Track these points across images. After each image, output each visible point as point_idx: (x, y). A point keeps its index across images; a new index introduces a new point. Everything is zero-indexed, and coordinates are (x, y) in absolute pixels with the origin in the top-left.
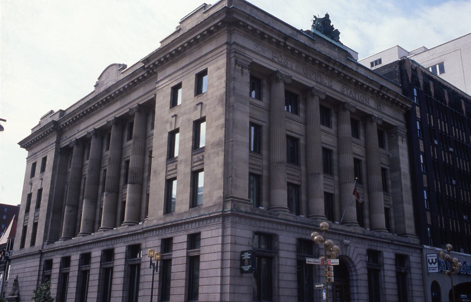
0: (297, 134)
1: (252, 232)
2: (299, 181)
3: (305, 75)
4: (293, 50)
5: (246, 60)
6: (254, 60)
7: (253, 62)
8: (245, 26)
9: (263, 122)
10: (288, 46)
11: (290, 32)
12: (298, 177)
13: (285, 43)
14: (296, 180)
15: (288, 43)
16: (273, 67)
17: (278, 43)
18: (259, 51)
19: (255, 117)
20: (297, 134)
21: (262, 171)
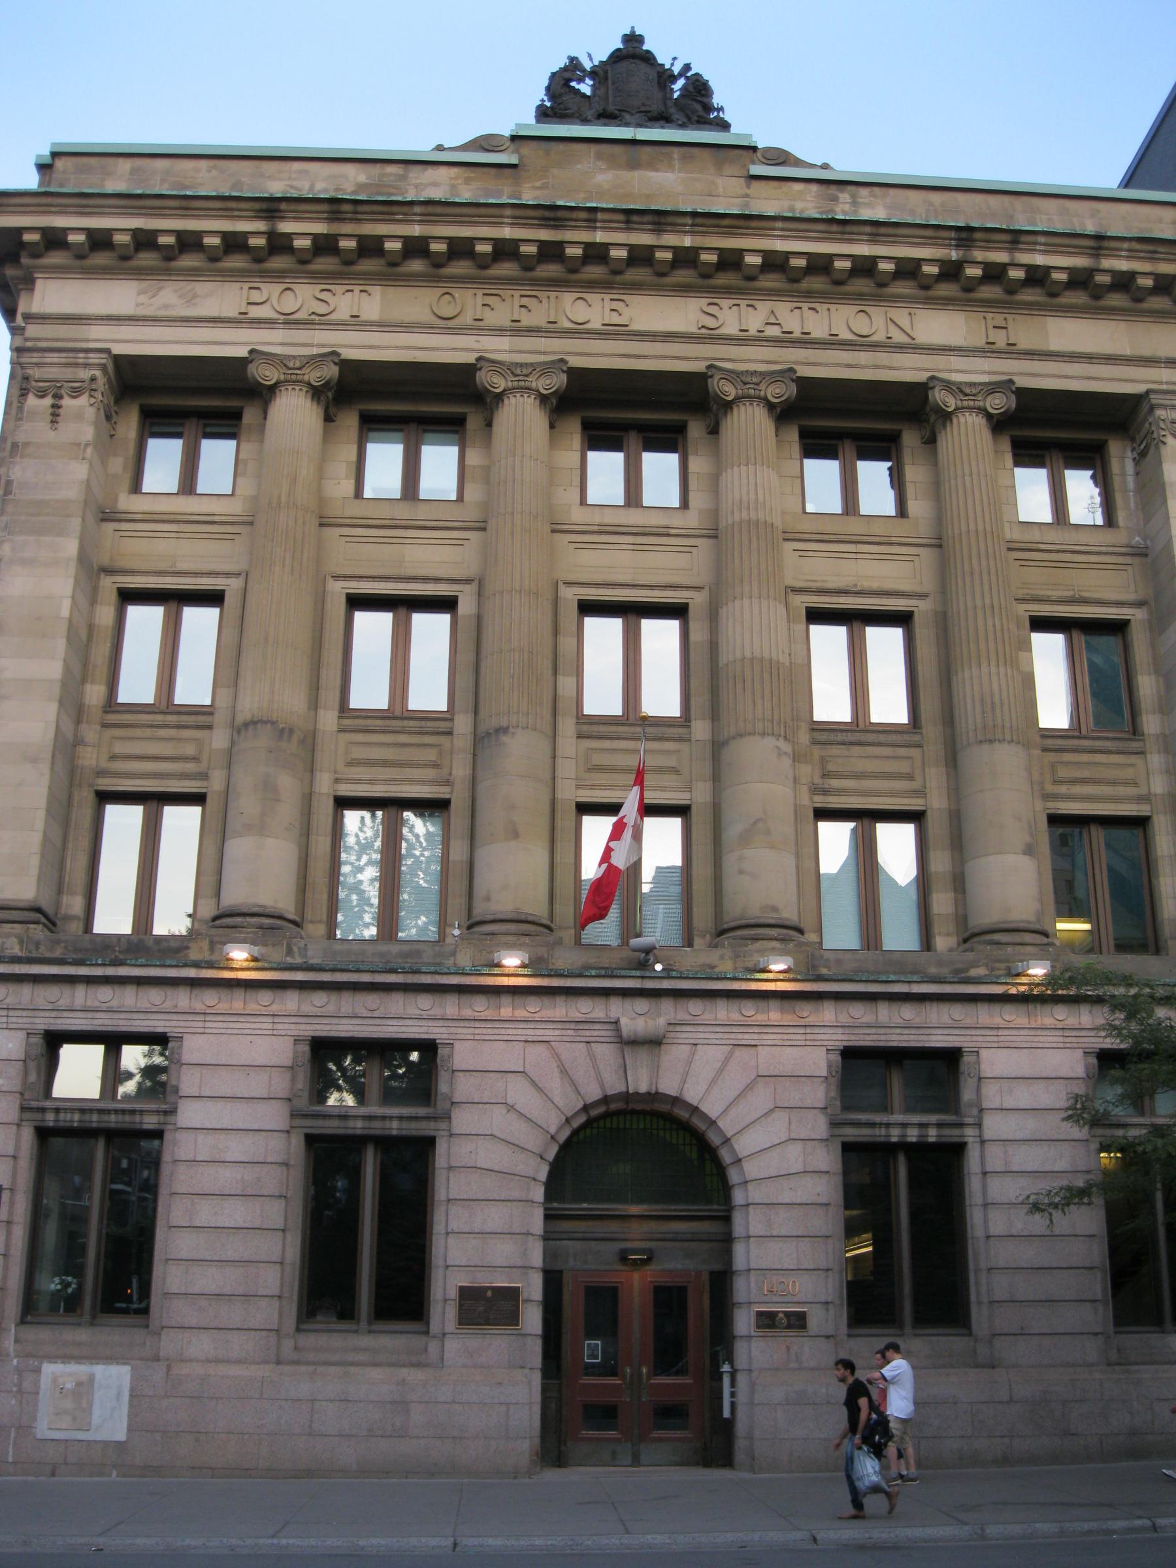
0: (437, 580)
1: (22, 1035)
2: (434, 782)
3: (446, 324)
4: (324, 246)
5: (76, 365)
6: (118, 349)
7: (119, 360)
8: (54, 240)
9: (228, 575)
10: (289, 236)
11: (362, 178)
12: (436, 766)
13: (272, 235)
14: (422, 782)
15: (286, 227)
16: (229, 344)
17: (234, 243)
18: (166, 306)
19: (182, 566)
20: (437, 580)
21: (204, 776)
